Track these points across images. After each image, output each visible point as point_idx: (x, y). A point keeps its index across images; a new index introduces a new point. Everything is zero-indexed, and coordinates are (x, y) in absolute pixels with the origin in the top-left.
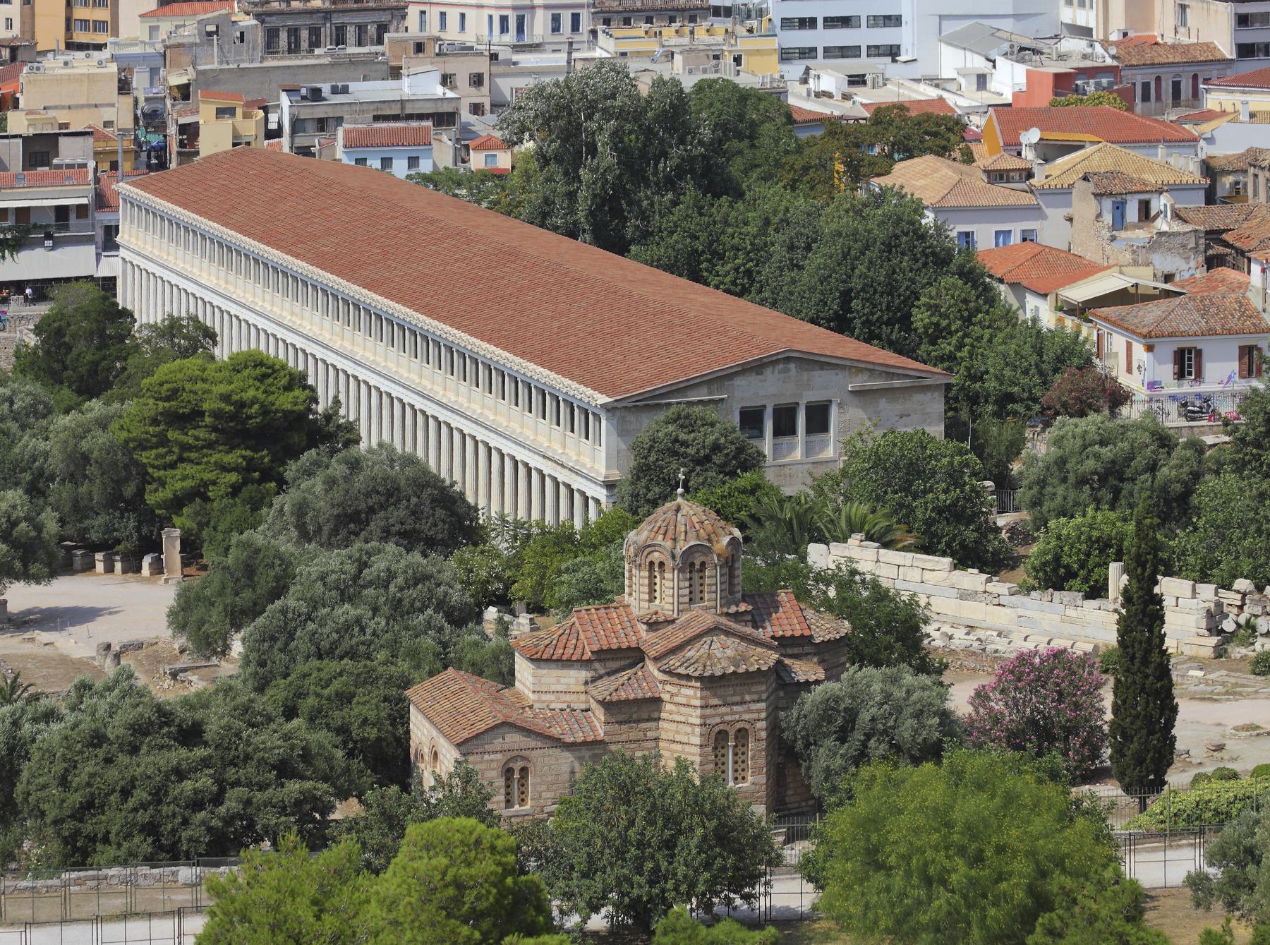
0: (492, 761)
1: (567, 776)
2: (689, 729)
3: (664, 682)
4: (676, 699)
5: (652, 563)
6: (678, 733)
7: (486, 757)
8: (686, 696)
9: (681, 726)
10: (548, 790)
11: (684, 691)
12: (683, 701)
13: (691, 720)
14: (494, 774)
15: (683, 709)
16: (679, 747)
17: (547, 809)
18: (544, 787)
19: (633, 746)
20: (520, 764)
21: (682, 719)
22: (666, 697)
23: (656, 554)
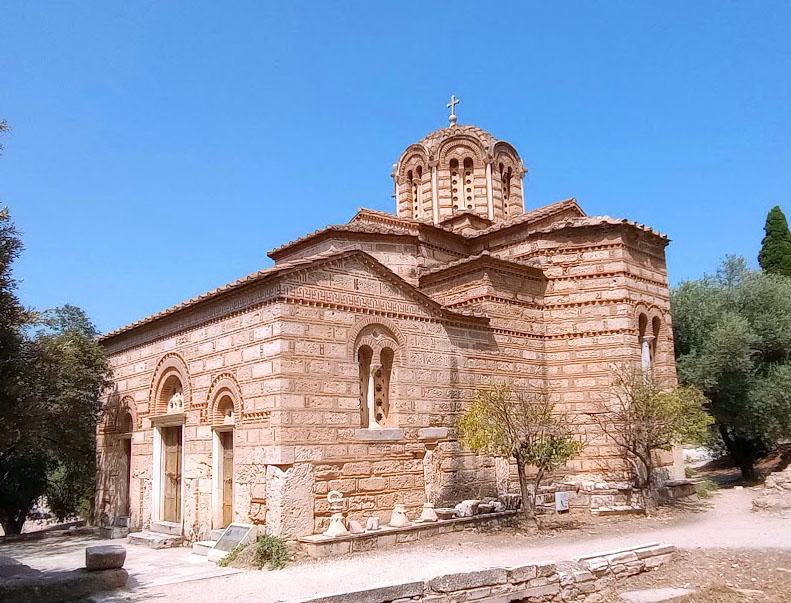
0: (338, 324)
1: (446, 377)
2: (605, 310)
3: (551, 251)
4: (573, 271)
5: (454, 163)
6: (583, 320)
7: (328, 313)
8: (598, 262)
9: (586, 309)
10: (423, 398)
11: (587, 256)
12: (591, 270)
13: (606, 295)
14: (341, 351)
15: (589, 283)
16: (587, 341)
17: (425, 433)
18: (417, 392)
19: (521, 341)
20: (377, 343)
21: (592, 297)
22: (550, 272)
23: (460, 150)
